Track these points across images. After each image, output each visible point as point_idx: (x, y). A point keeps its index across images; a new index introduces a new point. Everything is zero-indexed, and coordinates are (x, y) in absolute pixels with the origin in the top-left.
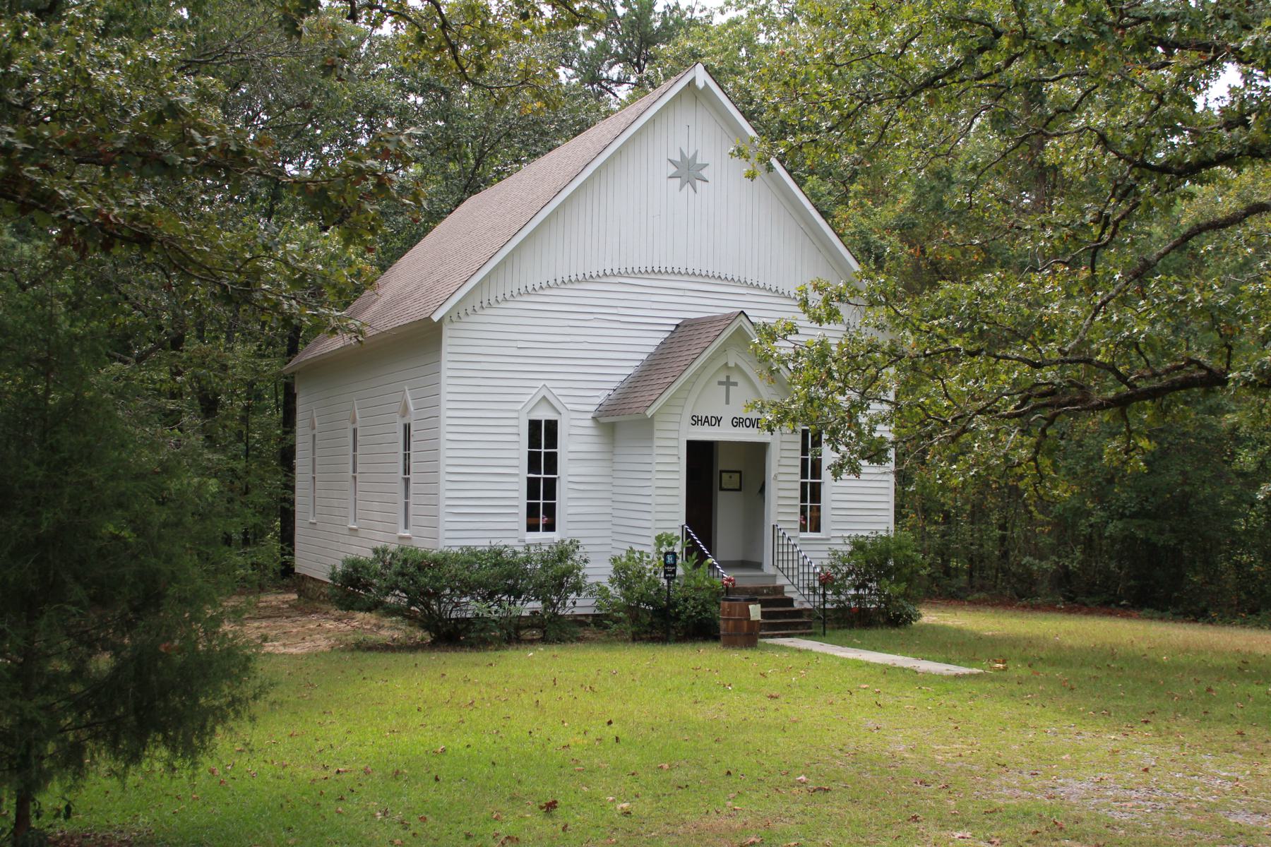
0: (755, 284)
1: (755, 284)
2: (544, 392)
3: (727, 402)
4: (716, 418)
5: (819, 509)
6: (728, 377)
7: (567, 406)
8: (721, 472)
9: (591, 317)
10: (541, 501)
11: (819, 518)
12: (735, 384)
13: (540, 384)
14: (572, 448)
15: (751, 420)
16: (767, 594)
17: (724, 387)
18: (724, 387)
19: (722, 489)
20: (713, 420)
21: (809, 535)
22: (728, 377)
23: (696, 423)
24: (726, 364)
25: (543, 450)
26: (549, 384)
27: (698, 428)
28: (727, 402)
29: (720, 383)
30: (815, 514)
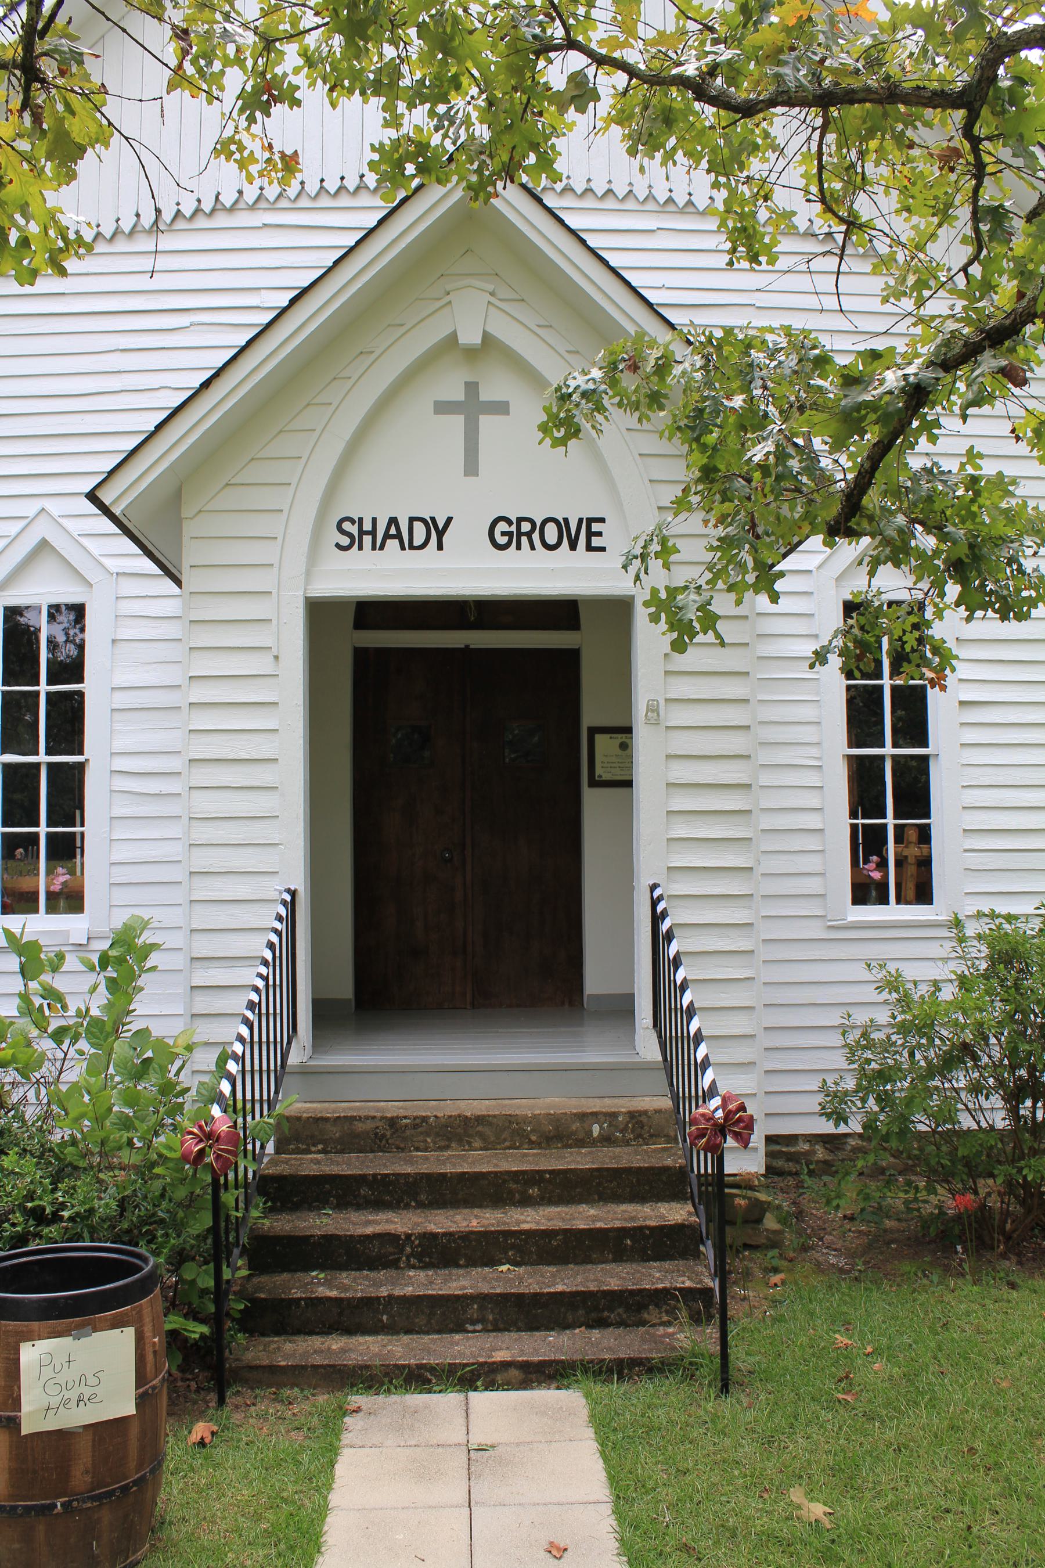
0: (681, 200)
1: (681, 200)
2: (41, 530)
3: (471, 467)
4: (430, 524)
5: (924, 835)
6: (472, 388)
7: (108, 562)
8: (593, 731)
9: (183, 320)
10: (43, 830)
11: (925, 863)
12: (501, 408)
13: (30, 508)
14: (122, 679)
15: (563, 526)
16: (607, 1140)
17: (458, 421)
18: (458, 421)
19: (594, 783)
20: (419, 529)
21: (894, 912)
22: (472, 388)
23: (354, 542)
24: (453, 337)
25: (43, 688)
26: (51, 505)
27: (364, 559)
28: (471, 467)
29: (443, 408)
30: (914, 851)
